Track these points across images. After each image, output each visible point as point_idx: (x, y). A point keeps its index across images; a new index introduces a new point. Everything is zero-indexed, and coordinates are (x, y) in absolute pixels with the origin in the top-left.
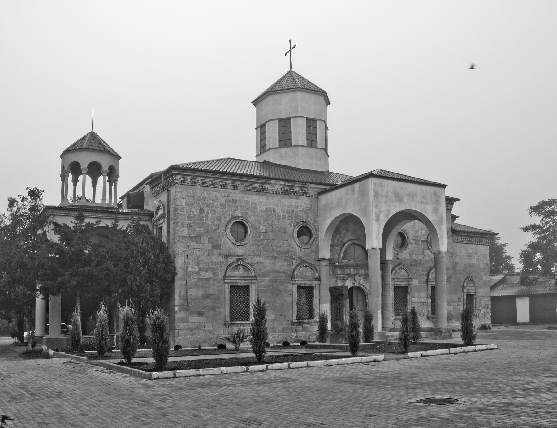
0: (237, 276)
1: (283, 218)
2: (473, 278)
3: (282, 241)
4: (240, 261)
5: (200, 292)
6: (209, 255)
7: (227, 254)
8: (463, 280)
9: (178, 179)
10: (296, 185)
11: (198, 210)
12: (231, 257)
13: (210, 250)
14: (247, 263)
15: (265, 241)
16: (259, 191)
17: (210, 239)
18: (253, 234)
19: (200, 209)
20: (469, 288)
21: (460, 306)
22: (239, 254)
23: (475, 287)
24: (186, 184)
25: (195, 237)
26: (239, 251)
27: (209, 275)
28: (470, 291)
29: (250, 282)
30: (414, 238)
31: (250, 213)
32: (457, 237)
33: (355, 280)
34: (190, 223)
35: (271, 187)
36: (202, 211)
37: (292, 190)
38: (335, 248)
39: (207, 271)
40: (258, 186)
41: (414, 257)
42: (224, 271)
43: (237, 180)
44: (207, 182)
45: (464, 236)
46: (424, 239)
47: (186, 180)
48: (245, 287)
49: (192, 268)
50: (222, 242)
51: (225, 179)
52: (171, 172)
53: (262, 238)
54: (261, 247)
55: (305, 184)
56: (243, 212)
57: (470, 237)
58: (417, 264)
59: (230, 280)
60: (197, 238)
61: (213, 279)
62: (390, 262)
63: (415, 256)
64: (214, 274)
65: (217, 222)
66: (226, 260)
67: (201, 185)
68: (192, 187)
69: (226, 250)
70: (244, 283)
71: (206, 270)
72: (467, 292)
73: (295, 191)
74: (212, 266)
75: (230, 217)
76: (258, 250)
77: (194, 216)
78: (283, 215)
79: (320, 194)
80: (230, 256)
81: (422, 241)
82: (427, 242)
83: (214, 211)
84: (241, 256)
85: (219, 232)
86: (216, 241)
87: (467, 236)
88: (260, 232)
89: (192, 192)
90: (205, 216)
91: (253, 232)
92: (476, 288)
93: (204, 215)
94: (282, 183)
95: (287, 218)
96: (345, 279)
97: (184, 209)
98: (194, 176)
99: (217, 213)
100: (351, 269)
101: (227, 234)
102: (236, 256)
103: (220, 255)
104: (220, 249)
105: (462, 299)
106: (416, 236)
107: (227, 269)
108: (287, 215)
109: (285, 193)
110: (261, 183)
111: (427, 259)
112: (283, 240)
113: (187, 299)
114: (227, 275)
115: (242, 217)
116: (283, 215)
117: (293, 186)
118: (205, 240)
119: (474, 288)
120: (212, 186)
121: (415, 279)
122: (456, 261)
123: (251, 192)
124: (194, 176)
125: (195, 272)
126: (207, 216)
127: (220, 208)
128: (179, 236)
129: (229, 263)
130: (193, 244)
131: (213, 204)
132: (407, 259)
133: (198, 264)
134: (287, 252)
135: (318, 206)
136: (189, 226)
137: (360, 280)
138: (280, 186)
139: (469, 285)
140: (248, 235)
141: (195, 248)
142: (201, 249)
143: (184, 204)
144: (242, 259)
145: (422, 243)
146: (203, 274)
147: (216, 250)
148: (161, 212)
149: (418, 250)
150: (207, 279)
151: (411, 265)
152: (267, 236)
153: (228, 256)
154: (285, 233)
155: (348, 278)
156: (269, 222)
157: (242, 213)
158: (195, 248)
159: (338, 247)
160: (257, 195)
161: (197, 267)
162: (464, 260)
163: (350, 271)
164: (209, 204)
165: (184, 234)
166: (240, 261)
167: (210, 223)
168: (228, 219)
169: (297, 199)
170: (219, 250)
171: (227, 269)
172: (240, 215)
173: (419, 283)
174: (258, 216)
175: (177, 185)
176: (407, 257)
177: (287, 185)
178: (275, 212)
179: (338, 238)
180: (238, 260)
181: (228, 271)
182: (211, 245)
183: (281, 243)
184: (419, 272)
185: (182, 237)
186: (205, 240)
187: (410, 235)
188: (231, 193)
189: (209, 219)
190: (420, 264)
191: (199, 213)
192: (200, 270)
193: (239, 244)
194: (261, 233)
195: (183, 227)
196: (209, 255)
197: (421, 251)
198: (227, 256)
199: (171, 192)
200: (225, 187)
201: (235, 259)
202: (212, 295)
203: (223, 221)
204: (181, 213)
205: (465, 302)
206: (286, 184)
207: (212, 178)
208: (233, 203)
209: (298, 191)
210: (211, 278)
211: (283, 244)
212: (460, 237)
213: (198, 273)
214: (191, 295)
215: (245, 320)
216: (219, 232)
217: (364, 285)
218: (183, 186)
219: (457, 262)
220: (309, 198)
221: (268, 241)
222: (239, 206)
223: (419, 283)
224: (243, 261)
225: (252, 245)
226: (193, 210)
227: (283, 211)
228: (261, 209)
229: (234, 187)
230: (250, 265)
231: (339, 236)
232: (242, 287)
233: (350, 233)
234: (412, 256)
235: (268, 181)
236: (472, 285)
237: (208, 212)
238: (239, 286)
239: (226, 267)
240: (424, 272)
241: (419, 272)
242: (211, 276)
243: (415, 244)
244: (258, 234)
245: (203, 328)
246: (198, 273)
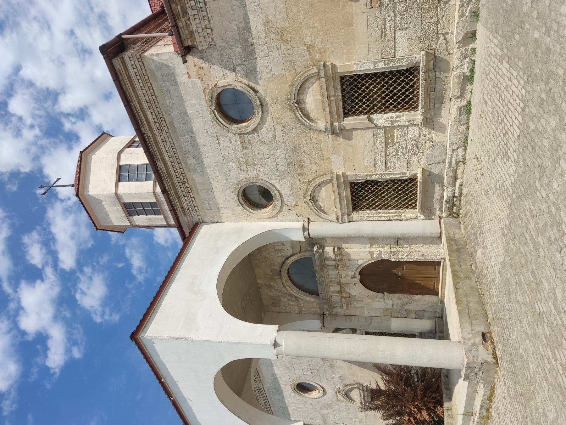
30: (244, 166)
32: (196, 35)
33: (349, 284)
38: (302, 305)
41: (282, 166)
45: (185, 13)
46: (239, 141)
58: (296, 158)
62: (306, 233)
63: (280, 164)
76: (326, 378)
81: (244, 147)
82: (243, 134)
96: (348, 296)
100: (331, 289)
106: (239, 162)
111: (279, 133)
118: (325, 412)
121: (330, 163)
122: (261, 28)
132: (292, 184)
137: (347, 275)
145: (248, 145)
149: (267, 156)
151: (302, 175)
155: (346, 292)
159: (300, 301)
163: (332, 291)
173: (339, 154)
176: (288, 183)
179: (286, 299)
184: (314, 152)
186: (325, 412)
187: (242, 177)
190: (294, 151)
197: (265, 149)
198: (338, 400)
203: (301, 398)
208: (278, 390)
217: (355, 268)
219: (265, 24)
223: (339, 154)
231: (282, 299)
233: (273, 284)
234: (282, 171)
240: (311, 140)
241: (314, 152)
243: (255, 164)
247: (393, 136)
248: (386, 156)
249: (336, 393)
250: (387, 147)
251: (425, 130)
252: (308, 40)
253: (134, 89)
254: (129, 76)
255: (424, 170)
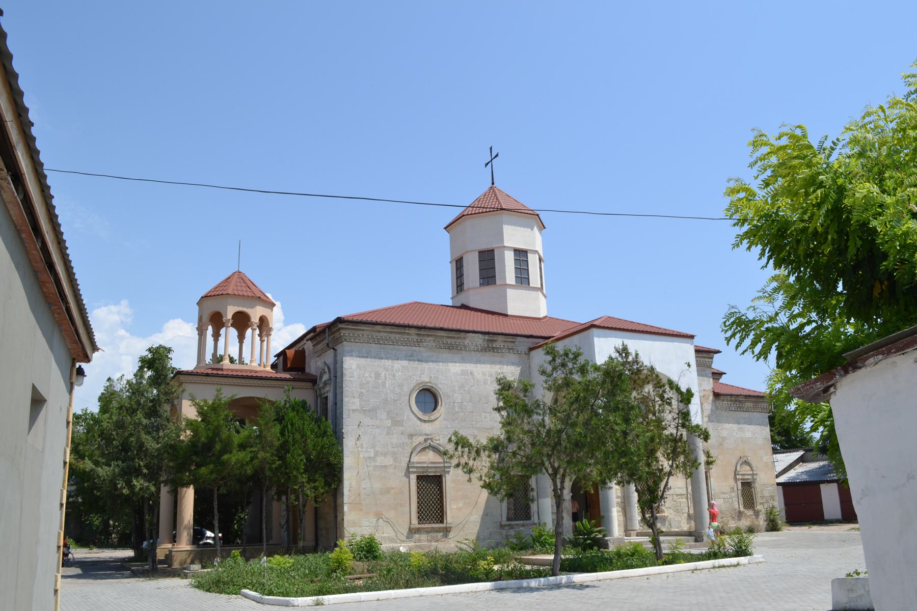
0: (424, 463)
1: (484, 382)
2: (749, 458)
3: (484, 415)
4: (429, 441)
5: (377, 485)
6: (388, 434)
7: (412, 433)
8: (734, 462)
9: (347, 335)
10: (500, 338)
11: (373, 375)
12: (416, 437)
13: (389, 428)
14: (438, 444)
15: (462, 414)
16: (450, 348)
17: (389, 413)
18: (445, 405)
19: (376, 374)
20: (743, 473)
21: (734, 499)
22: (428, 432)
23: (752, 470)
24: (357, 341)
25: (370, 411)
26: (427, 428)
27: (389, 461)
28: (747, 477)
29: (442, 469)
31: (440, 377)
34: (362, 393)
35: (467, 342)
36: (378, 376)
37: (494, 346)
39: (386, 457)
40: (449, 341)
42: (409, 456)
43: (423, 335)
44: (383, 338)
45: (731, 401)
47: (356, 336)
48: (436, 476)
49: (366, 452)
50: (405, 418)
51: (407, 333)
52: (337, 326)
53: (457, 410)
54: (456, 422)
55: (511, 337)
56: (431, 377)
57: (740, 402)
59: (417, 467)
60: (371, 412)
61: (393, 466)
64: (395, 460)
65: (397, 390)
66: (410, 441)
67: (376, 342)
68: (365, 345)
69: (410, 426)
70: (435, 472)
71: (385, 454)
72: (742, 479)
73: (498, 346)
74: (392, 449)
75: (413, 383)
76: (452, 427)
77: (368, 382)
78: (484, 379)
79: (531, 349)
80: (416, 435)
83: (394, 375)
84: (431, 435)
85: (401, 404)
86: (397, 415)
87: (736, 401)
88: (454, 403)
89: (364, 352)
90: (382, 382)
91: (446, 403)
92: (754, 472)
93: (380, 381)
94: (480, 335)
95: (489, 382)
97: (355, 373)
98: (367, 330)
99: (397, 378)
101: (411, 405)
102: (422, 435)
103: (402, 434)
104: (402, 426)
105: (735, 489)
107: (412, 453)
108: (489, 378)
109: (485, 350)
110: (454, 338)
112: (485, 412)
113: (359, 495)
114: (412, 460)
115: (430, 382)
116: (484, 379)
117: (495, 341)
118: (382, 415)
119: (751, 472)
120: (390, 343)
123: (440, 350)
124: (367, 330)
125: (370, 458)
126: (385, 383)
127: (402, 372)
128: (349, 410)
129: (414, 445)
130: (366, 421)
131: (393, 367)
133: (373, 447)
134: (492, 429)
135: (530, 366)
136: (361, 395)
138: (479, 340)
139: (743, 469)
140: (439, 407)
141: (369, 426)
142: (377, 427)
143: (354, 366)
144: (431, 439)
146: (380, 461)
147: (396, 427)
148: (326, 377)
150: (386, 466)
152: (464, 407)
153: (413, 435)
154: (488, 403)
156: (466, 389)
157: (431, 377)
158: (369, 426)
160: (449, 353)
161: (372, 451)
162: (735, 434)
164: (386, 366)
165: (354, 408)
166: (429, 441)
167: (388, 392)
168: (412, 386)
169: (502, 357)
170: (401, 428)
171: (412, 453)
172: (427, 380)
174: (451, 381)
175: (345, 343)
177: (488, 340)
178: (474, 376)
180: (426, 440)
181: (413, 455)
182: (390, 421)
183: (483, 417)
185: (354, 411)
188: (415, 351)
189: (387, 386)
191: (373, 379)
192: (376, 454)
193: (426, 418)
194: (456, 404)
195: (354, 397)
196: (388, 434)
198: (411, 436)
199: (338, 351)
200: (407, 343)
201: (421, 439)
202: (393, 488)
203: (406, 389)
204: (351, 379)
205: (740, 492)
206: (487, 337)
207: (391, 332)
209: (502, 347)
210: (391, 465)
211: (485, 417)
212: (725, 402)
213: (373, 459)
214: (365, 489)
215: (437, 522)
216: (401, 404)
218: (353, 343)
220: (517, 356)
221: (465, 414)
222: (426, 369)
224: (432, 441)
225: (445, 420)
226: (367, 375)
227: (484, 374)
228: (455, 371)
229: (418, 343)
230: (442, 447)
232: (432, 476)
235: (462, 335)
236: (748, 468)
237: (386, 378)
238: (429, 476)
239: (410, 450)
242: (391, 462)
244: (452, 404)
245: (382, 535)
246: (373, 459)
247: (682, 498)
248: (673, 495)
249: (427, 435)
250: (677, 495)
251: (686, 515)
252: (720, 457)
253: (701, 357)
254: (705, 357)
255: (667, 517)
